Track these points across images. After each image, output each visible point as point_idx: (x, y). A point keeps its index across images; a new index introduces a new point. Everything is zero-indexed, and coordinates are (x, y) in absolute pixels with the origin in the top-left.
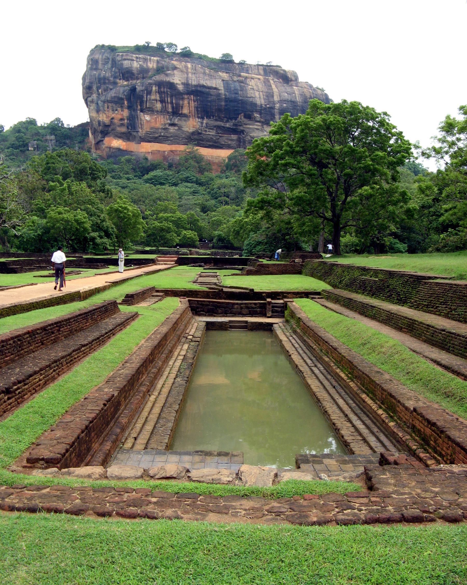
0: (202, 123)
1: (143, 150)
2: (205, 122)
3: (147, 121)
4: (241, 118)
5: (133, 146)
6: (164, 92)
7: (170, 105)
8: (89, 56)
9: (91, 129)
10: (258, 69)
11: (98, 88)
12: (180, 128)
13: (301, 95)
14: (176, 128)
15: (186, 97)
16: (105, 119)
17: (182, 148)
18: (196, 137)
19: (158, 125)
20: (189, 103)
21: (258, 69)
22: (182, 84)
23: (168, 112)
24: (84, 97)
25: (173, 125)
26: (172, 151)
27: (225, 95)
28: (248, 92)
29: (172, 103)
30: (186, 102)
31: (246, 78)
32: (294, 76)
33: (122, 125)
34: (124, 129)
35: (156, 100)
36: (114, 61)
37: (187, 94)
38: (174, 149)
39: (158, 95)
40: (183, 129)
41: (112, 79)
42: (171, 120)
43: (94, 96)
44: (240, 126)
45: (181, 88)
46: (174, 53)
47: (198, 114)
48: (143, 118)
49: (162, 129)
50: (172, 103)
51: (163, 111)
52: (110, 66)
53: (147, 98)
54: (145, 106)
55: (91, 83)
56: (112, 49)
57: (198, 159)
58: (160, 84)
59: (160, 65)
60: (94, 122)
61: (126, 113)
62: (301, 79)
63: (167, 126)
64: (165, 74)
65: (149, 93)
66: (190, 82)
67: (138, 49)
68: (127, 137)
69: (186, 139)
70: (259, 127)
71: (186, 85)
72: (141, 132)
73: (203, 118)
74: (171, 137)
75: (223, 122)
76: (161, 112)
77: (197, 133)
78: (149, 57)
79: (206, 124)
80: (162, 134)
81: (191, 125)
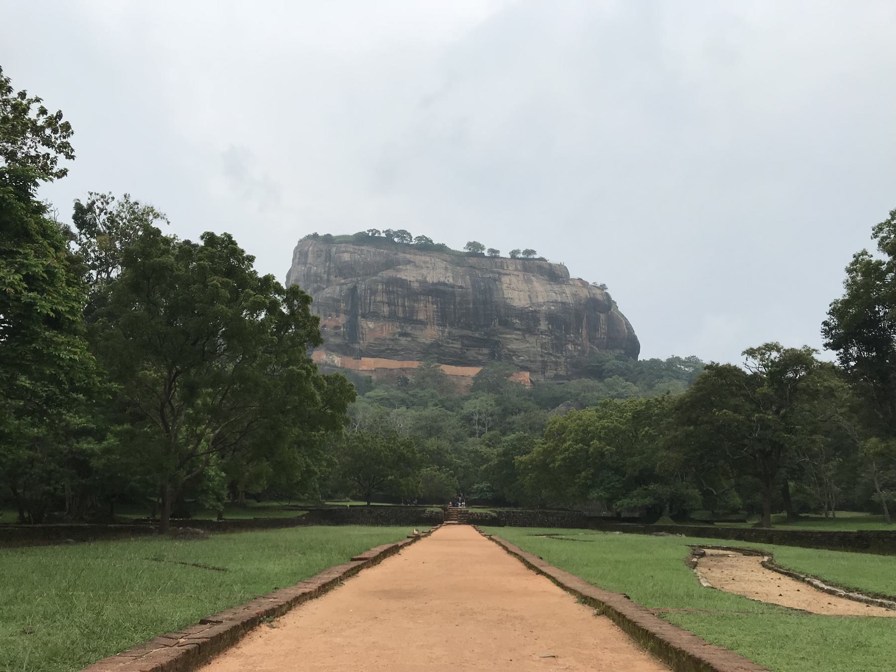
0: (443, 332)
1: (365, 368)
5: (350, 363)
6: (393, 292)
7: (401, 309)
8: (296, 248)
12: (414, 339)
13: (574, 295)
14: (409, 339)
17: (415, 364)
19: (384, 334)
23: (398, 318)
25: (405, 335)
26: (403, 369)
31: (500, 274)
33: (337, 335)
34: (338, 341)
35: (383, 302)
36: (329, 252)
38: (405, 366)
40: (419, 340)
42: (402, 328)
44: (493, 335)
45: (415, 285)
46: (408, 245)
48: (365, 326)
49: (390, 339)
50: (404, 306)
51: (392, 317)
52: (323, 258)
55: (296, 280)
56: (328, 239)
57: (440, 379)
61: (342, 319)
62: (573, 275)
63: (397, 336)
65: (374, 293)
67: (362, 239)
68: (345, 350)
70: (520, 337)
71: (423, 282)
72: (362, 345)
74: (403, 350)
77: (436, 345)
79: (449, 333)
81: (430, 334)
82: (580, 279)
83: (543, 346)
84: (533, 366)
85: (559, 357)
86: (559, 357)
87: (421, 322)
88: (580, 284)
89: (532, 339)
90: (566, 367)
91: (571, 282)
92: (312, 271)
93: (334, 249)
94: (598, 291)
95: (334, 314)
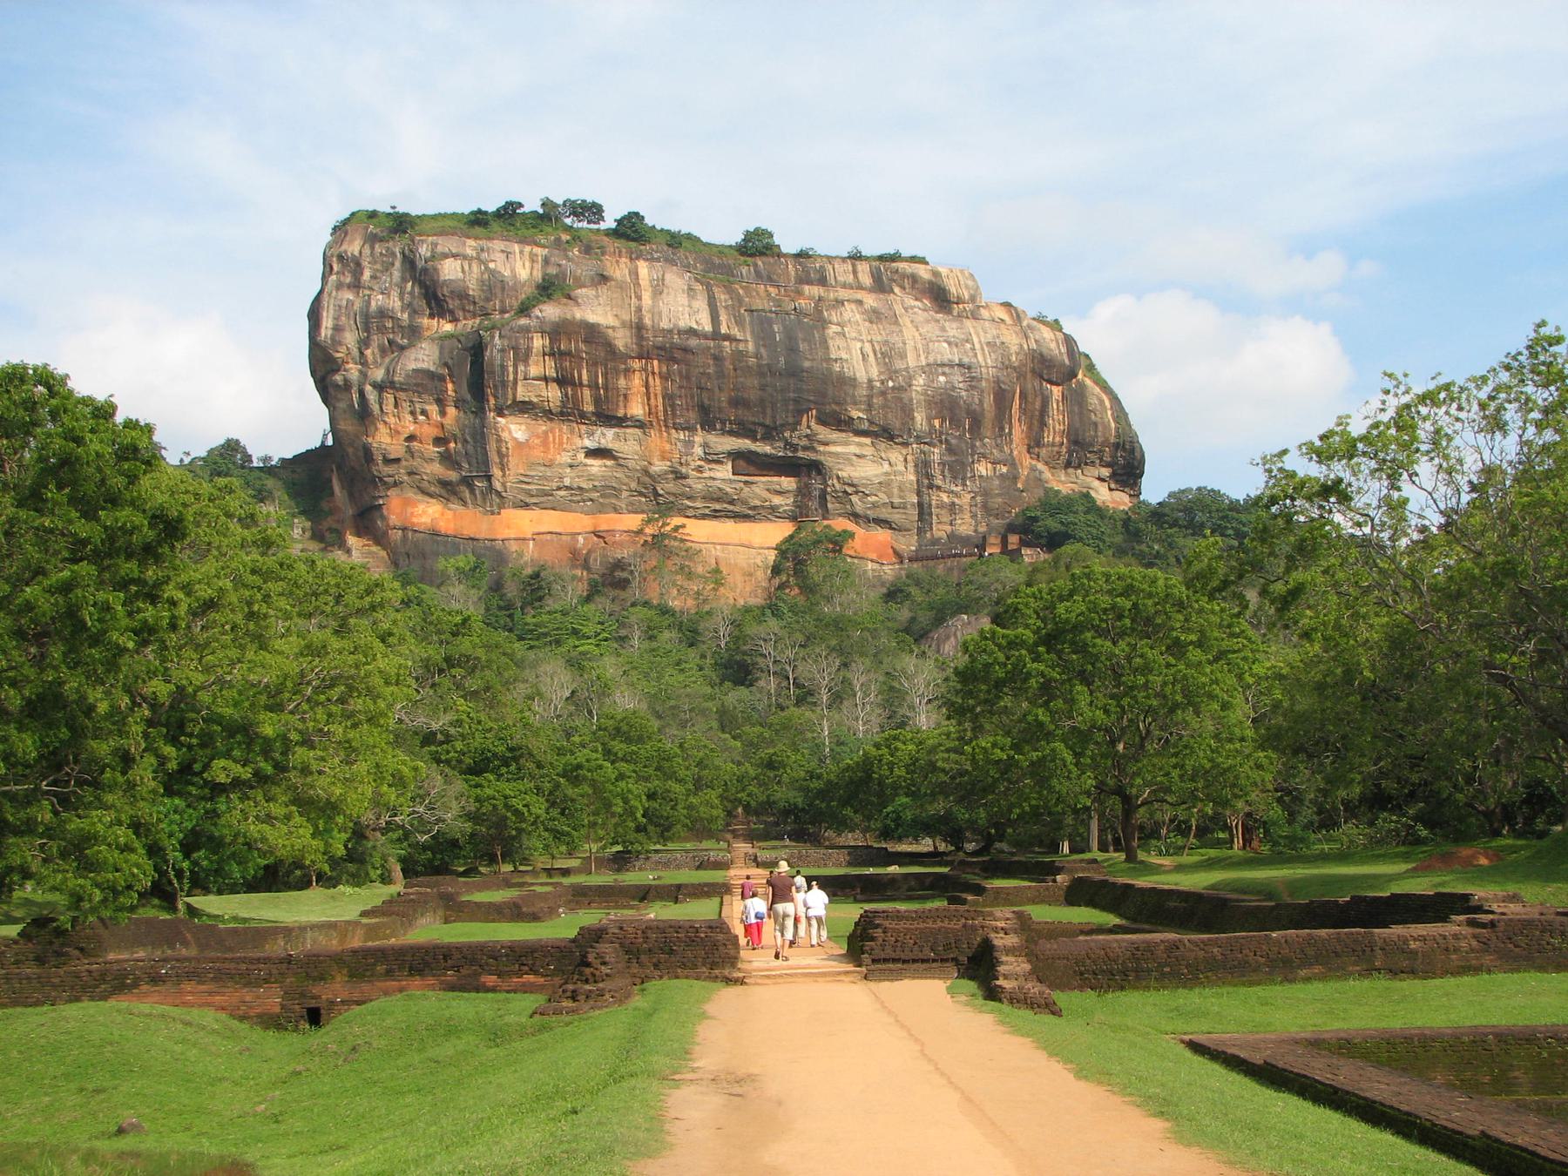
2: (698, 439)
3: (519, 445)
4: (810, 424)
6: (569, 353)
7: (587, 392)
8: (329, 246)
9: (339, 468)
10: (855, 272)
11: (364, 343)
14: (609, 463)
15: (636, 364)
16: (388, 440)
18: (671, 486)
20: (647, 386)
21: (855, 272)
22: (624, 324)
23: (583, 415)
24: (313, 373)
26: (597, 534)
27: (757, 356)
28: (831, 343)
29: (594, 386)
30: (637, 381)
32: (967, 287)
35: (546, 379)
36: (409, 262)
37: (640, 357)
38: (603, 527)
39: (550, 363)
40: (631, 464)
41: (406, 316)
43: (353, 371)
45: (622, 340)
47: (674, 415)
48: (505, 435)
51: (569, 413)
52: (397, 275)
53: (516, 373)
54: (510, 396)
55: (337, 329)
58: (556, 332)
59: (552, 270)
60: (350, 450)
62: (991, 294)
64: (569, 297)
65: (523, 356)
66: (647, 321)
69: (641, 494)
73: (690, 429)
75: (755, 439)
76: (562, 413)
78: (516, 247)
79: (705, 445)
80: (567, 482)
82: (1007, 305)
83: (923, 468)
84: (896, 517)
85: (957, 495)
86: (957, 495)
87: (641, 425)
88: (1006, 317)
89: (896, 455)
90: (974, 516)
91: (984, 313)
92: (373, 304)
93: (424, 251)
94: (1047, 334)
95: (433, 409)
